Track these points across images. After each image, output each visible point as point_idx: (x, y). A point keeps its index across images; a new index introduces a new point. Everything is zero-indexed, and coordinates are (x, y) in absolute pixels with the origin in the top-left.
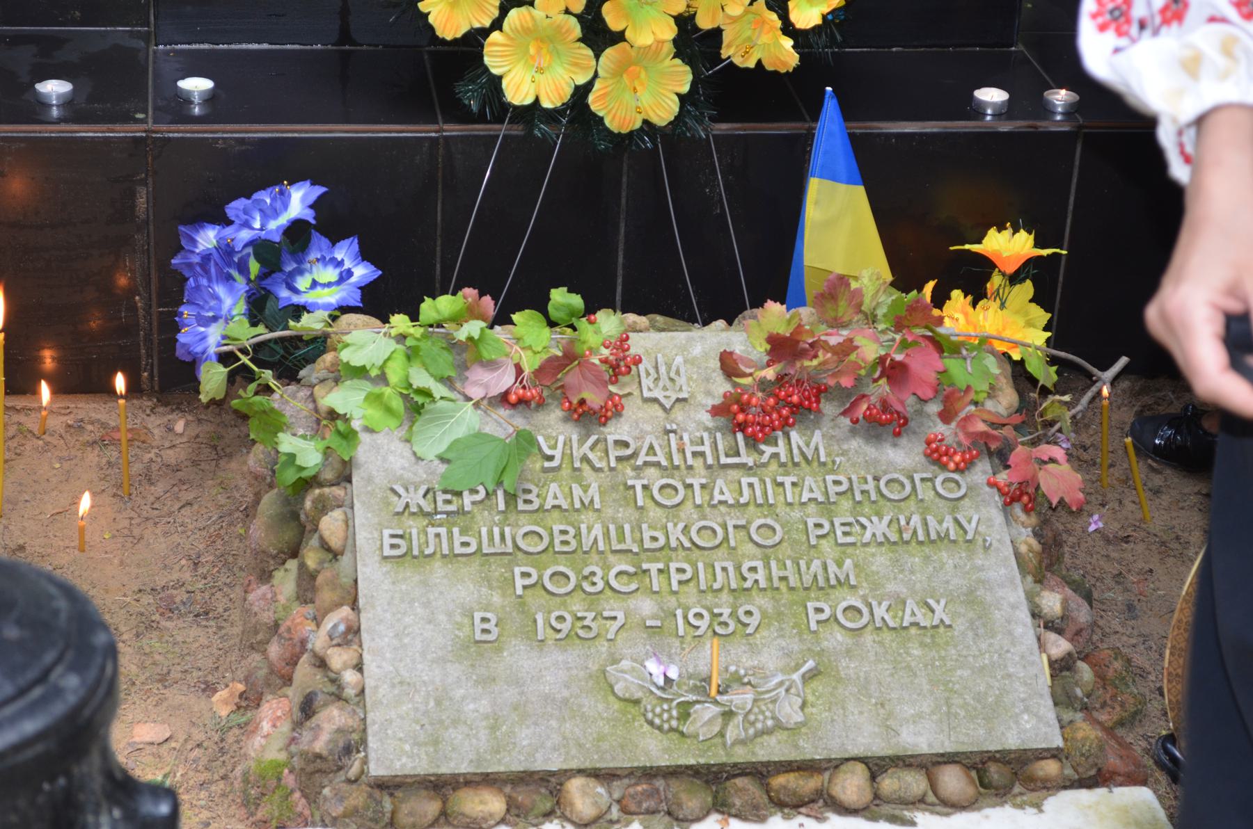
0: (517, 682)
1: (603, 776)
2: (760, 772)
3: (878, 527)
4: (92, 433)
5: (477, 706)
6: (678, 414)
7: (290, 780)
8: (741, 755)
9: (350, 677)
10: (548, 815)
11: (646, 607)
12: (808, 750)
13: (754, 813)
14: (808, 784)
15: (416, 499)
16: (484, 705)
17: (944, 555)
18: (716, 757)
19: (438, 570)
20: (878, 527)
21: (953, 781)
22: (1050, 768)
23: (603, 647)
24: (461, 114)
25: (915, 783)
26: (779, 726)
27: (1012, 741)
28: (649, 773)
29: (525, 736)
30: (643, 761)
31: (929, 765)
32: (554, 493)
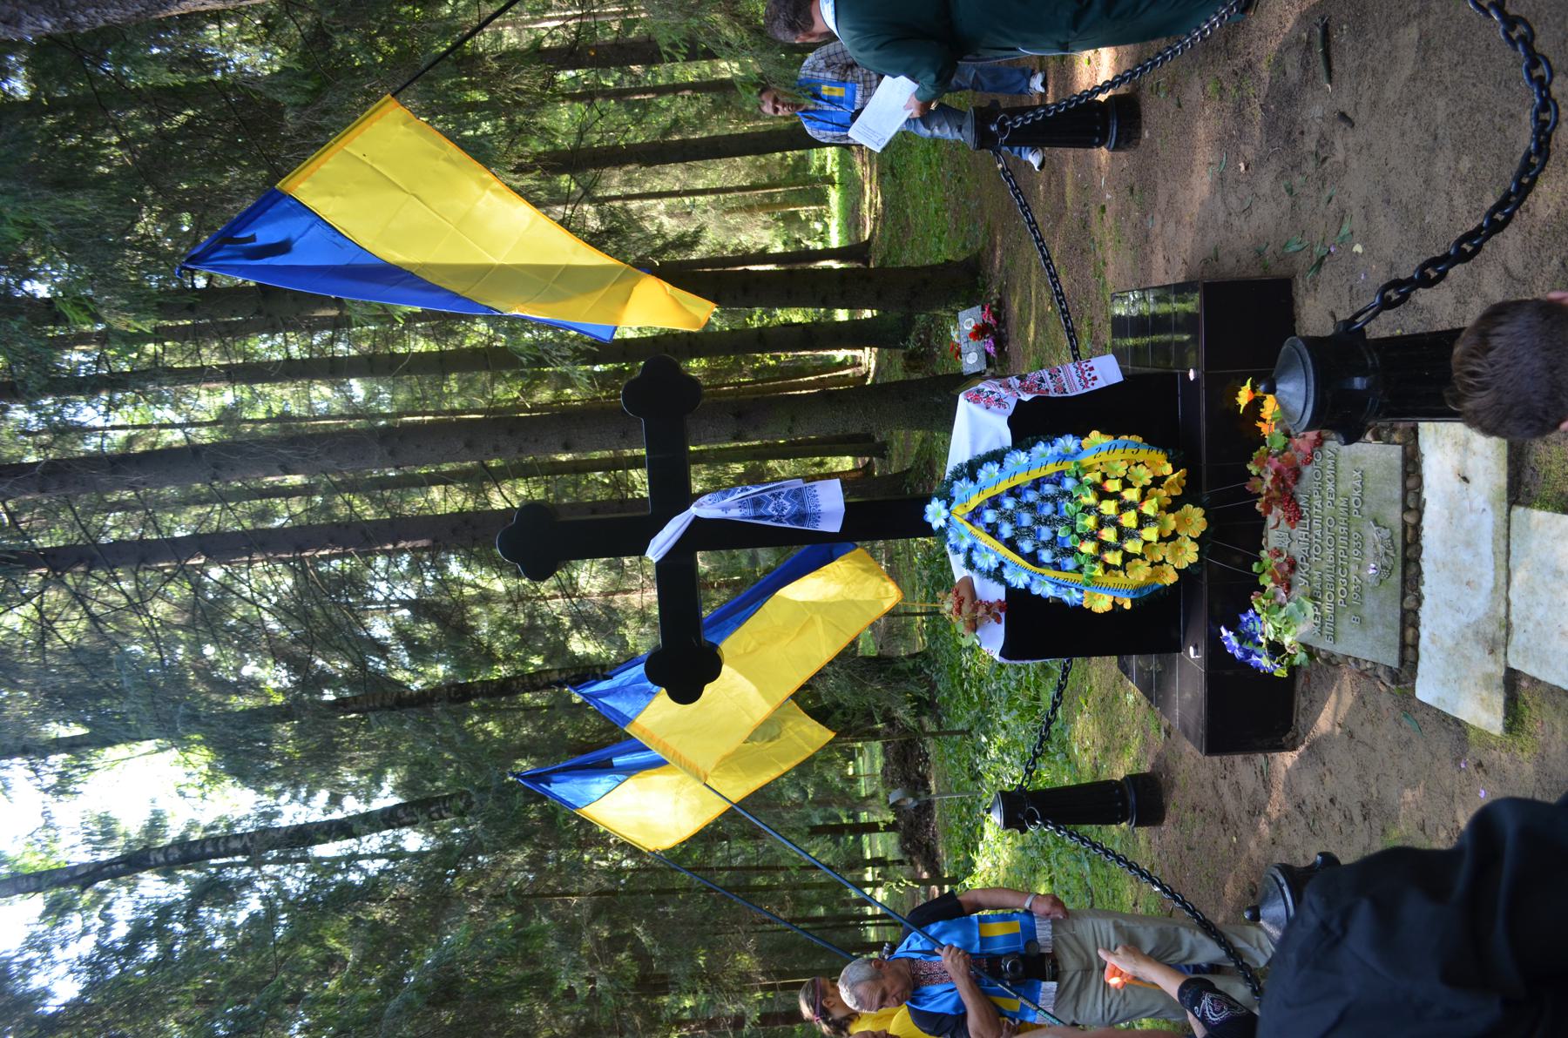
0: (1373, 615)
1: (1404, 596)
2: (1406, 546)
3: (1330, 486)
4: (1305, 688)
5: (1380, 630)
6: (1294, 537)
7: (1401, 686)
8: (1399, 551)
9: (1368, 666)
10: (1416, 613)
11: (1353, 568)
12: (1398, 530)
13: (1419, 550)
14: (1410, 532)
15: (1317, 629)
16: (1380, 627)
17: (1340, 465)
18: (1399, 559)
19: (1339, 628)
20: (1330, 486)
21: (1411, 483)
22: (1409, 449)
23: (1364, 585)
24: (1199, 576)
25: (1411, 497)
26: (1391, 538)
27: (1399, 463)
28: (1404, 581)
29: (1390, 618)
30: (1399, 584)
31: (1405, 491)
32: (1316, 585)
